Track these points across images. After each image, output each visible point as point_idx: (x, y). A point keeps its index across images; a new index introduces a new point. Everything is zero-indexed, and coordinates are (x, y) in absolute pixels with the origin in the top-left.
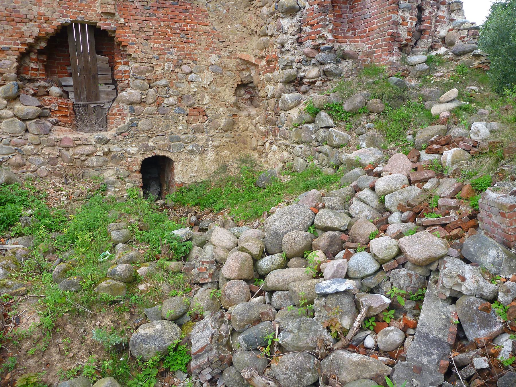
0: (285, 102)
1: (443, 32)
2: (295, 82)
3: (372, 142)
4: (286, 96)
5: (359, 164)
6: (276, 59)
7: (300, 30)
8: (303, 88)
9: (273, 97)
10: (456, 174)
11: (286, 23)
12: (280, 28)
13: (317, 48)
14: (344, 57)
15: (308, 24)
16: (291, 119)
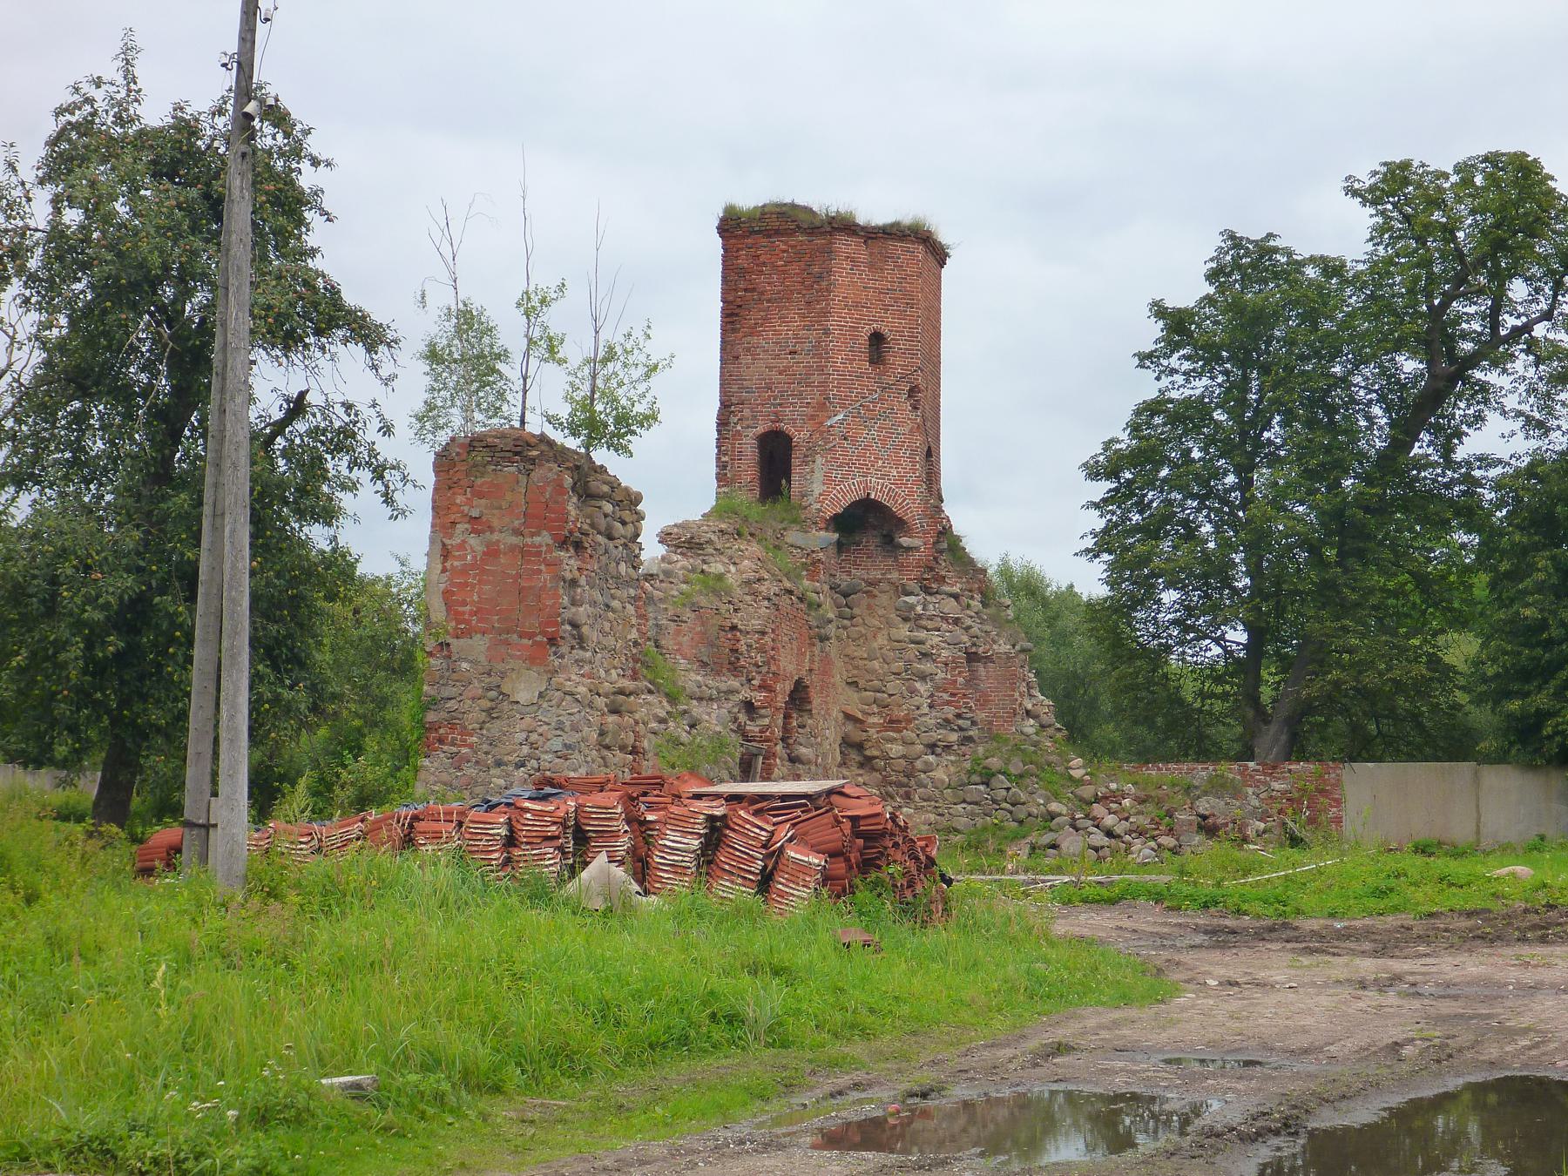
0: (926, 763)
1: (1029, 706)
2: (932, 747)
3: (1048, 800)
4: (931, 758)
5: (1060, 815)
6: (909, 721)
7: (932, 696)
8: (939, 750)
9: (904, 757)
10: (1140, 813)
11: (918, 685)
12: (913, 691)
13: (959, 716)
14: (974, 723)
15: (945, 691)
16: (943, 782)
